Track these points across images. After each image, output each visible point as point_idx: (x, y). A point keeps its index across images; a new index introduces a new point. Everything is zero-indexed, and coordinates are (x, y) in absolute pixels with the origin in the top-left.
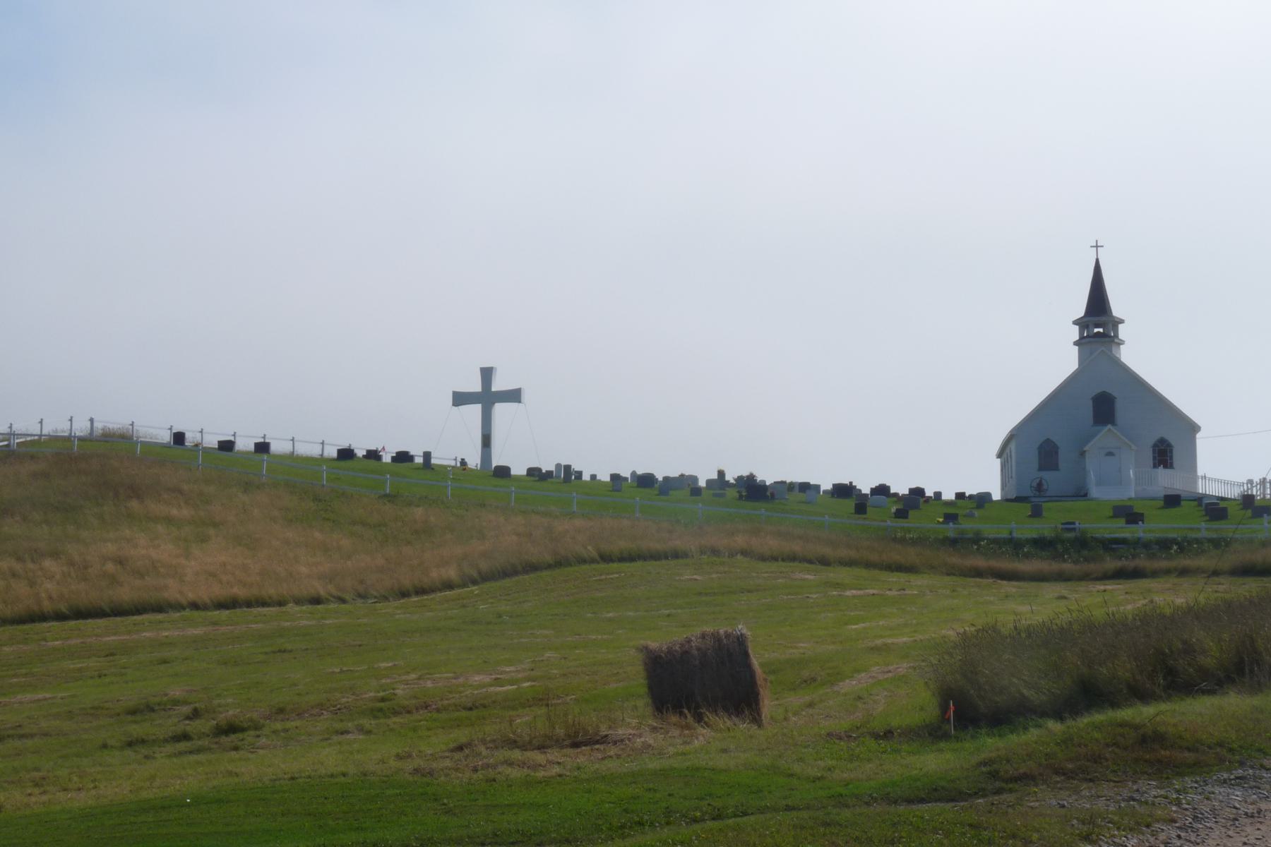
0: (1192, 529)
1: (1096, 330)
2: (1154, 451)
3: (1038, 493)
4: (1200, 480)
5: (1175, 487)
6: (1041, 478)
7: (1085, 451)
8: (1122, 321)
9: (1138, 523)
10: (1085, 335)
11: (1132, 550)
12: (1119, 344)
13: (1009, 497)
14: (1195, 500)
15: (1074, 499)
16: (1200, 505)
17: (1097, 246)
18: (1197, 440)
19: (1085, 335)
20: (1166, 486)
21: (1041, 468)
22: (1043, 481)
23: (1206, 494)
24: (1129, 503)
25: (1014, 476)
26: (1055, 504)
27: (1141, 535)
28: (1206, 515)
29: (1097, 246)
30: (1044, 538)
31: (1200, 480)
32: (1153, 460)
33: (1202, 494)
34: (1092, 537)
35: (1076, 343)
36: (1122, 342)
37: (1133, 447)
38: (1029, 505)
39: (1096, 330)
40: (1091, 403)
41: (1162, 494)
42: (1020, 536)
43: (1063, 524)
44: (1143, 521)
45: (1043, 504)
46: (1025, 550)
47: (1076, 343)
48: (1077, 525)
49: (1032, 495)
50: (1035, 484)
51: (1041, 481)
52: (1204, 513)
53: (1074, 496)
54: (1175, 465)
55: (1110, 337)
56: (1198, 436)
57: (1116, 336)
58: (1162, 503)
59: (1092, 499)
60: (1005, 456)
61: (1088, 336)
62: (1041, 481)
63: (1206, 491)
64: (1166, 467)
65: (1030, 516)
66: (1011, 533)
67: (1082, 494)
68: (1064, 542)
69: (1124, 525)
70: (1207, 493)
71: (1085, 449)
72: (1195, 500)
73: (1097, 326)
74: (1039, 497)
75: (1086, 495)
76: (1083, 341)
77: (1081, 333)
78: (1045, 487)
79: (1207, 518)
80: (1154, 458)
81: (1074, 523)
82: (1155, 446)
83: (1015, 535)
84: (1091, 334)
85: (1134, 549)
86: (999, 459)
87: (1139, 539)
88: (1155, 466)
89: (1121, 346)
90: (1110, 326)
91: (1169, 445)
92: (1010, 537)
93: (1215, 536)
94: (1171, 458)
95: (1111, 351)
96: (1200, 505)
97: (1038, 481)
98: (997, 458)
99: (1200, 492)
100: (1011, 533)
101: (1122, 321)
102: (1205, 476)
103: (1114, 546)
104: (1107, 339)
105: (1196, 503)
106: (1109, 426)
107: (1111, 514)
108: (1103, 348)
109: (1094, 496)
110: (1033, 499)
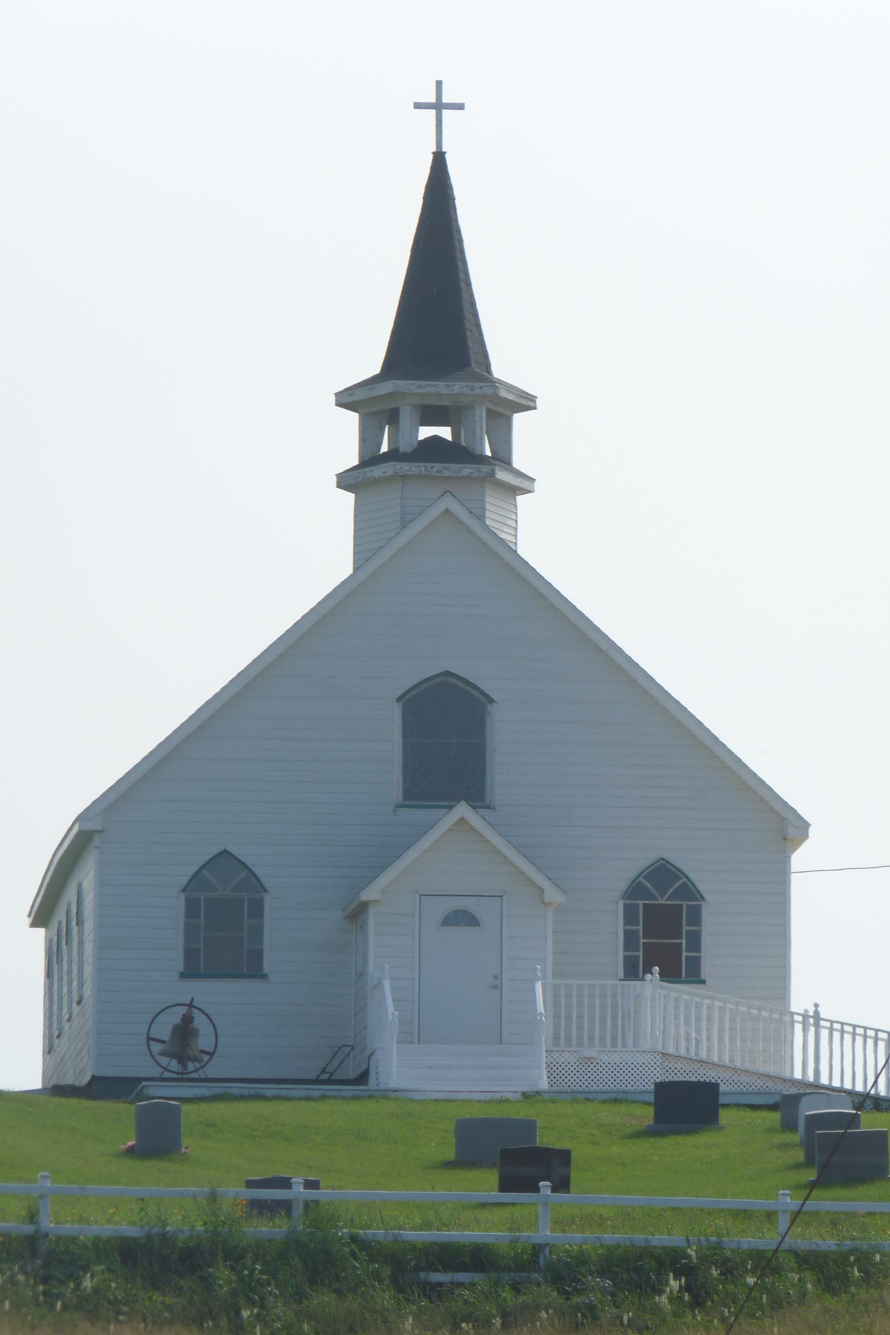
0: (744, 1215)
1: (425, 432)
2: (630, 916)
3: (174, 1065)
4: (798, 1028)
5: (704, 1055)
6: (191, 1005)
7: (363, 907)
8: (526, 403)
9: (537, 1190)
10: (384, 448)
11: (507, 1294)
12: (514, 491)
13: (69, 1080)
14: (773, 1107)
15: (316, 1090)
16: (789, 1125)
17: (439, 106)
18: (793, 877)
19: (384, 448)
20: (671, 1049)
21: (190, 972)
22: (199, 1021)
23: (816, 1086)
24: (522, 1112)
25: (87, 991)
26: (242, 1107)
27: (545, 1233)
28: (809, 1162)
29: (439, 106)
30: (164, 1235)
31: (798, 1028)
32: (627, 948)
33: (803, 1083)
34: (354, 1238)
35: (345, 481)
36: (523, 484)
37: (552, 895)
38: (132, 1108)
39: (425, 432)
40: (396, 712)
41: (646, 1083)
42: (68, 1228)
43: (250, 1184)
44: (562, 1185)
45: (186, 1108)
46: (88, 1283)
47: (345, 481)
48: (298, 1189)
49: (156, 1072)
50: (164, 1030)
51: (188, 1019)
52: (800, 1155)
53: (316, 1081)
54: (706, 970)
55: (481, 459)
56: (799, 859)
57: (503, 457)
58: (646, 1115)
59: (386, 1095)
60: (60, 915)
61: (394, 455)
62: (188, 1019)
63: (817, 1073)
64: (671, 974)
65: (131, 1152)
66: (32, 1217)
67: (352, 1075)
68: (242, 1257)
69: (495, 1195)
70: (824, 1081)
71: (365, 896)
72: (773, 1107)
73: (431, 416)
74: (182, 1078)
75: (363, 1078)
76: (377, 471)
77: (368, 438)
78: (205, 1041)
79: (811, 1175)
80: (630, 941)
81: (285, 1183)
82: (635, 891)
83: (47, 1224)
84: (405, 447)
85: (516, 1289)
86: (41, 932)
87: (537, 1249)
88: (632, 971)
89: (520, 499)
90: (481, 413)
91: (690, 892)
92: (29, 1229)
93: (828, 1243)
94: (695, 942)
95: (481, 518)
96: (789, 1125)
97: (175, 1017)
98: (35, 924)
99: (798, 1075)
100: (32, 1217)
101: (526, 403)
102: (817, 1016)
103: (436, 1277)
104: (466, 470)
105: (775, 1117)
106: (462, 810)
107: (450, 1154)
108: (448, 502)
109: (393, 1085)
110: (154, 1089)
